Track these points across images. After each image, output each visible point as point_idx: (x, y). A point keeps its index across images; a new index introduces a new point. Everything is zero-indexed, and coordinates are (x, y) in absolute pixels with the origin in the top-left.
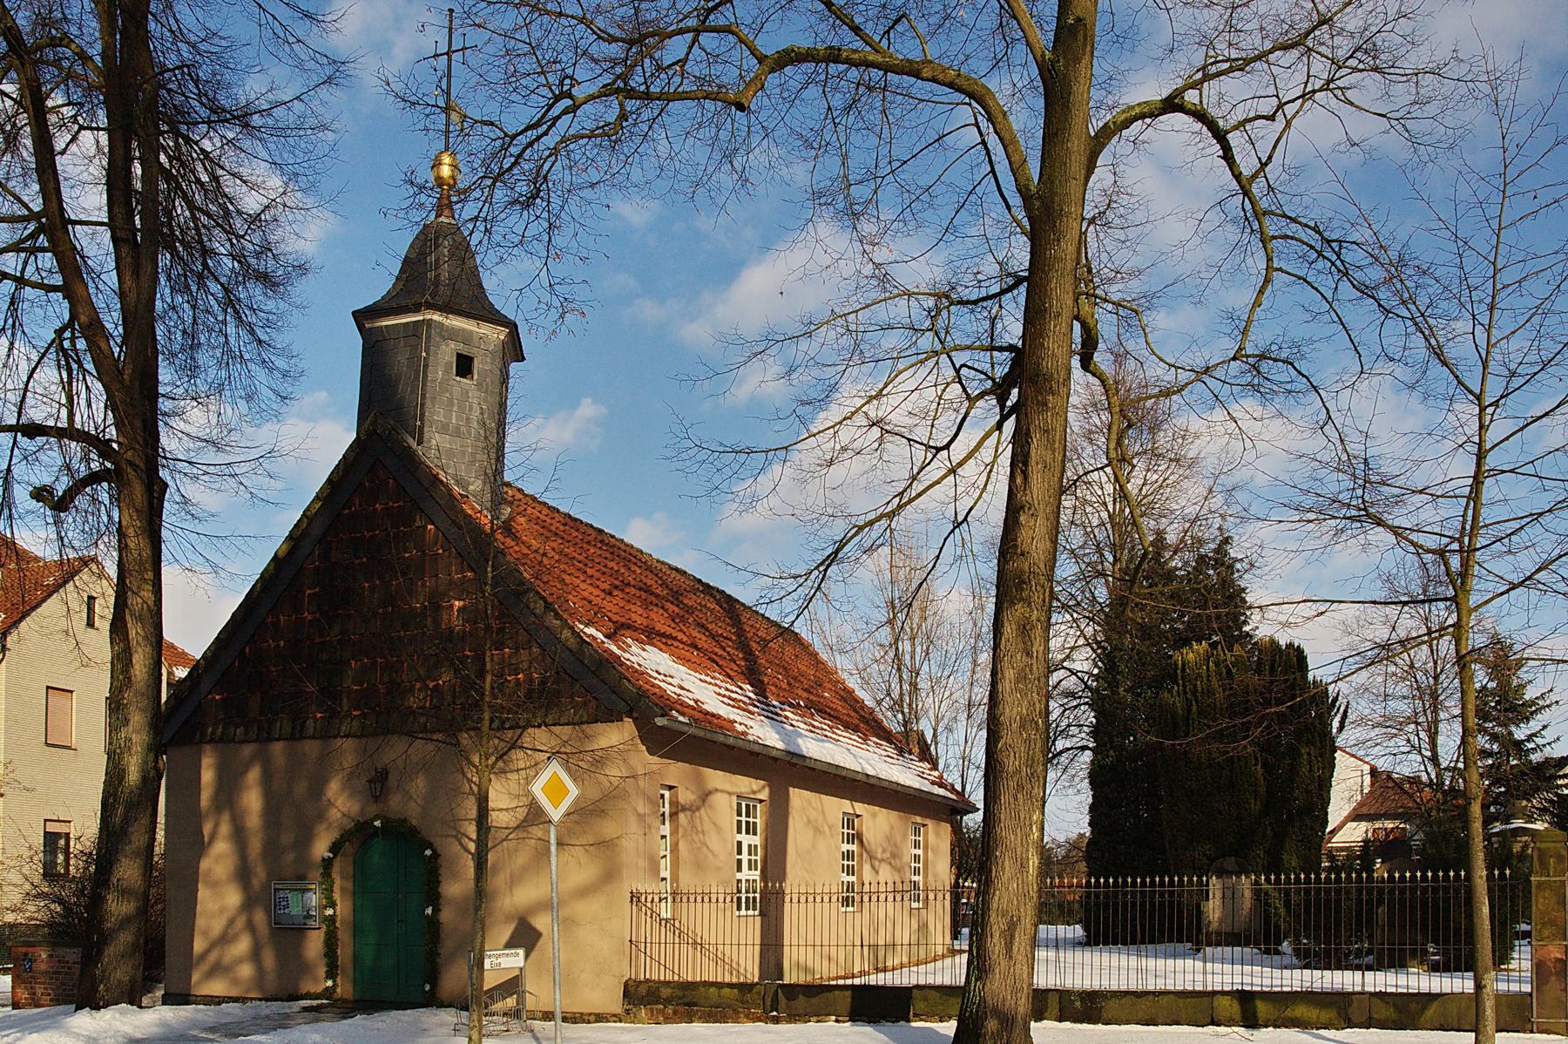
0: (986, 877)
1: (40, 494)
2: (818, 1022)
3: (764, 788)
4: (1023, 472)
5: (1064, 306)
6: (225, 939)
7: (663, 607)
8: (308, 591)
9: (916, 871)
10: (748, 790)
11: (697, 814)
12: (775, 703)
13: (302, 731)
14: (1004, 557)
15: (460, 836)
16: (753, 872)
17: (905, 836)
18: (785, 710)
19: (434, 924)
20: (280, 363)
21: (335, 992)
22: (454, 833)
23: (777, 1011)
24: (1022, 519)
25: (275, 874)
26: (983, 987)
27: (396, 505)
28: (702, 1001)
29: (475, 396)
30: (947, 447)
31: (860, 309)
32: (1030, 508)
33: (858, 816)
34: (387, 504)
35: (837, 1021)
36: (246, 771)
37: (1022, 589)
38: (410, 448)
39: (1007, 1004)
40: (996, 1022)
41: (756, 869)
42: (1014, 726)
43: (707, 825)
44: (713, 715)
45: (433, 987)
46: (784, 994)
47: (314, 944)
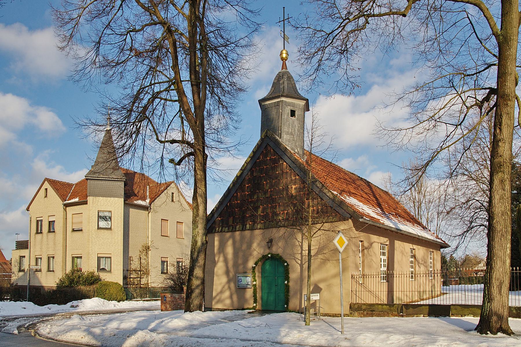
0: (491, 267)
1: (172, 161)
2: (417, 317)
3: (388, 240)
4: (500, 128)
5: (513, 71)
6: (221, 292)
7: (351, 185)
8: (247, 185)
9: (431, 267)
10: (384, 241)
11: (370, 250)
12: (387, 214)
13: (245, 228)
14: (493, 157)
15: (295, 259)
16: (385, 268)
17: (428, 257)
18: (390, 216)
19: (287, 287)
20: (235, 118)
21: (256, 307)
22: (294, 258)
23: (402, 313)
24: (500, 144)
25: (237, 272)
26: (491, 305)
27: (273, 157)
28: (376, 310)
29: (296, 123)
30: (460, 124)
31: (434, 81)
32: (503, 140)
33: (414, 249)
34: (271, 157)
35: (424, 316)
36: (227, 241)
37: (501, 168)
38: (277, 139)
39: (500, 311)
40: (496, 317)
41: (386, 267)
42: (500, 215)
43: (372, 253)
44: (374, 218)
45: (288, 306)
46: (404, 307)
47: (249, 293)
